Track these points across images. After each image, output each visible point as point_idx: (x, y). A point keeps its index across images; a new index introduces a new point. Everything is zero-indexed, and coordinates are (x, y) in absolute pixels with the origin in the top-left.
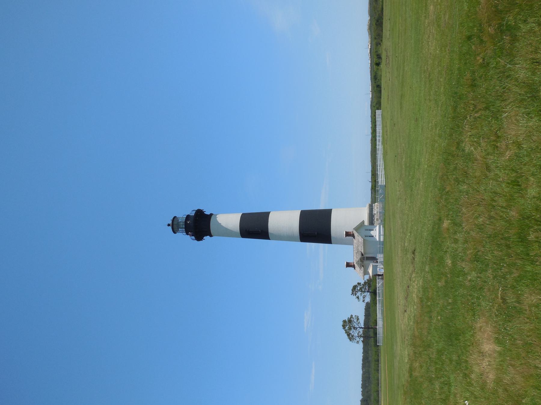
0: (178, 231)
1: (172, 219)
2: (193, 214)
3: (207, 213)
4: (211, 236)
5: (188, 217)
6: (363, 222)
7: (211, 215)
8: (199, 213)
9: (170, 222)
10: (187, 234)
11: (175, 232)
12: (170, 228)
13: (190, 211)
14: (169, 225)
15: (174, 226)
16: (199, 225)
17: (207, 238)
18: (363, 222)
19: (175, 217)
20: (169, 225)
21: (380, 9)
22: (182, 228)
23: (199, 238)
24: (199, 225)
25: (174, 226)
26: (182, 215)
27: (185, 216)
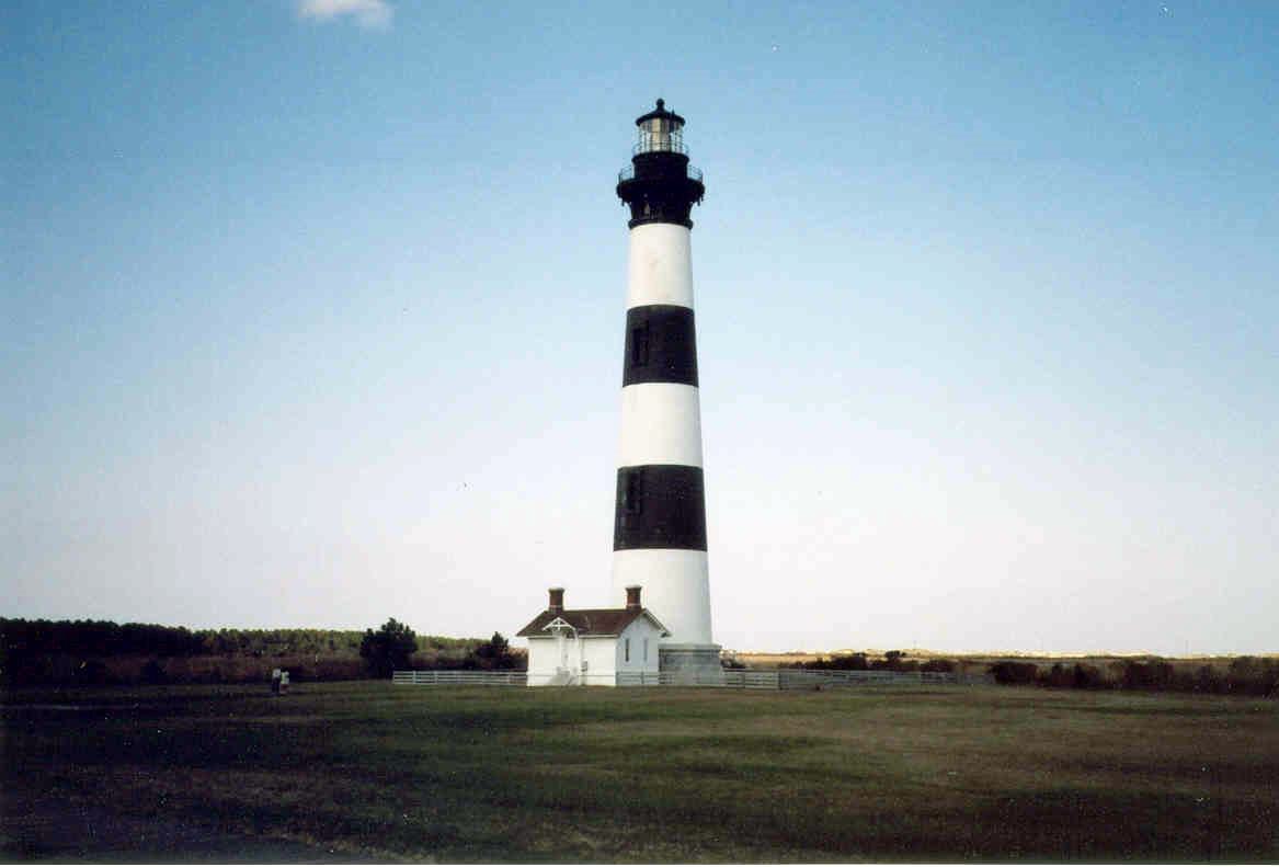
1: (677, 113)
2: (692, 174)
3: (696, 212)
4: (632, 225)
5: (682, 160)
7: (689, 225)
8: (696, 191)
9: (668, 108)
11: (640, 122)
14: (660, 103)
17: (625, 212)
19: (681, 121)
20: (660, 103)
21: (812, 676)
23: (626, 191)
24: (662, 189)
26: (687, 142)
27: (684, 152)
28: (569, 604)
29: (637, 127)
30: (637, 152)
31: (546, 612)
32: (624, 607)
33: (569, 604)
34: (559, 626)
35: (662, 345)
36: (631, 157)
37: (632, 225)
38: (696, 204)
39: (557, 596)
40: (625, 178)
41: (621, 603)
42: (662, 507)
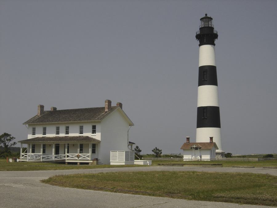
1: (211, 17)
3: (216, 42)
5: (212, 29)
7: (214, 45)
8: (216, 36)
9: (208, 16)
10: (200, 29)
11: (201, 19)
12: (204, 16)
13: (216, 29)
14: (206, 15)
15: (207, 19)
16: (207, 36)
17: (198, 43)
20: (206, 15)
22: (204, 25)
23: (198, 37)
25: (207, 19)
29: (200, 21)
30: (200, 27)
36: (199, 28)
37: (200, 45)
38: (216, 39)
40: (198, 34)
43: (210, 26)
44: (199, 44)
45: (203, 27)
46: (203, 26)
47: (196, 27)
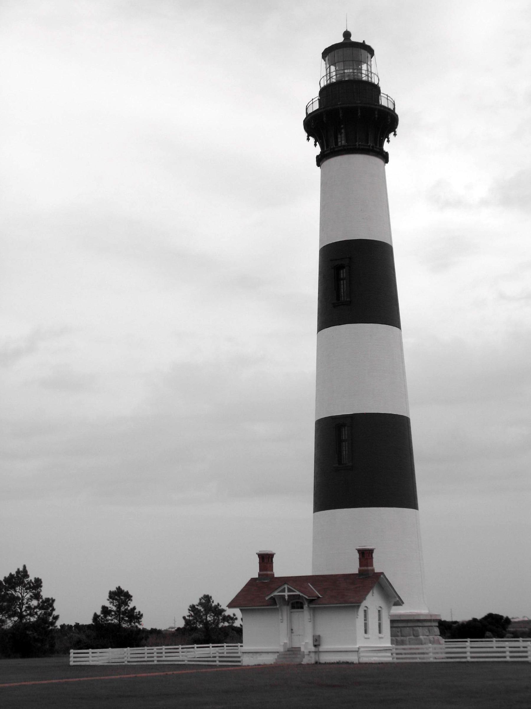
0: (332, 63)
1: (367, 43)
6: (399, 603)
8: (388, 121)
9: (353, 39)
10: (324, 92)
11: (326, 53)
12: (340, 39)
14: (347, 35)
15: (348, 52)
18: (399, 603)
20: (347, 35)
25: (348, 52)
28: (280, 570)
30: (324, 83)
31: (253, 580)
32: (356, 571)
33: (280, 570)
34: (286, 594)
35: (356, 282)
39: (266, 560)
40: (310, 111)
41: (352, 566)
42: (363, 459)
43: (365, 78)
44: (320, 150)
45: (339, 83)
46: (334, 80)
47: (307, 83)
